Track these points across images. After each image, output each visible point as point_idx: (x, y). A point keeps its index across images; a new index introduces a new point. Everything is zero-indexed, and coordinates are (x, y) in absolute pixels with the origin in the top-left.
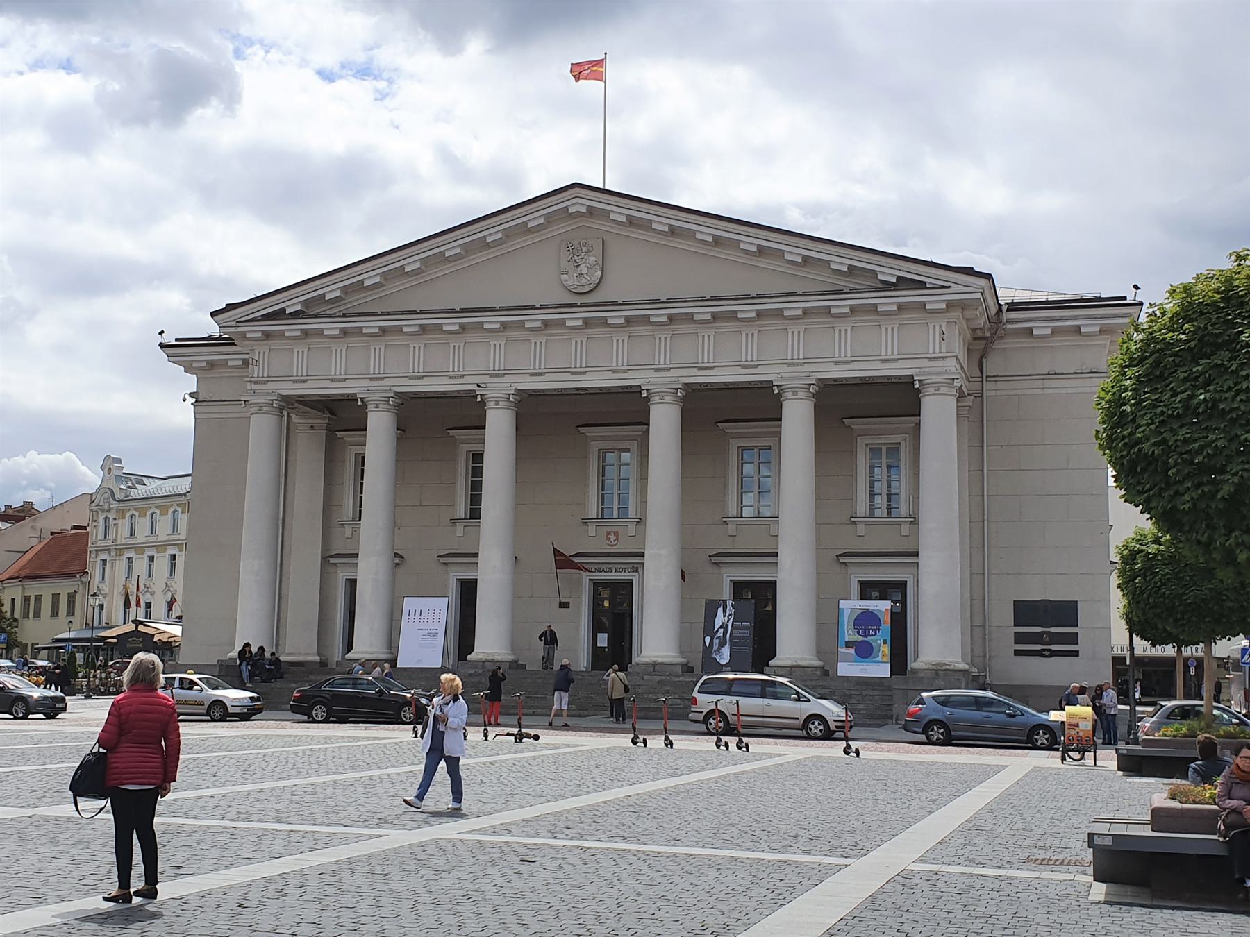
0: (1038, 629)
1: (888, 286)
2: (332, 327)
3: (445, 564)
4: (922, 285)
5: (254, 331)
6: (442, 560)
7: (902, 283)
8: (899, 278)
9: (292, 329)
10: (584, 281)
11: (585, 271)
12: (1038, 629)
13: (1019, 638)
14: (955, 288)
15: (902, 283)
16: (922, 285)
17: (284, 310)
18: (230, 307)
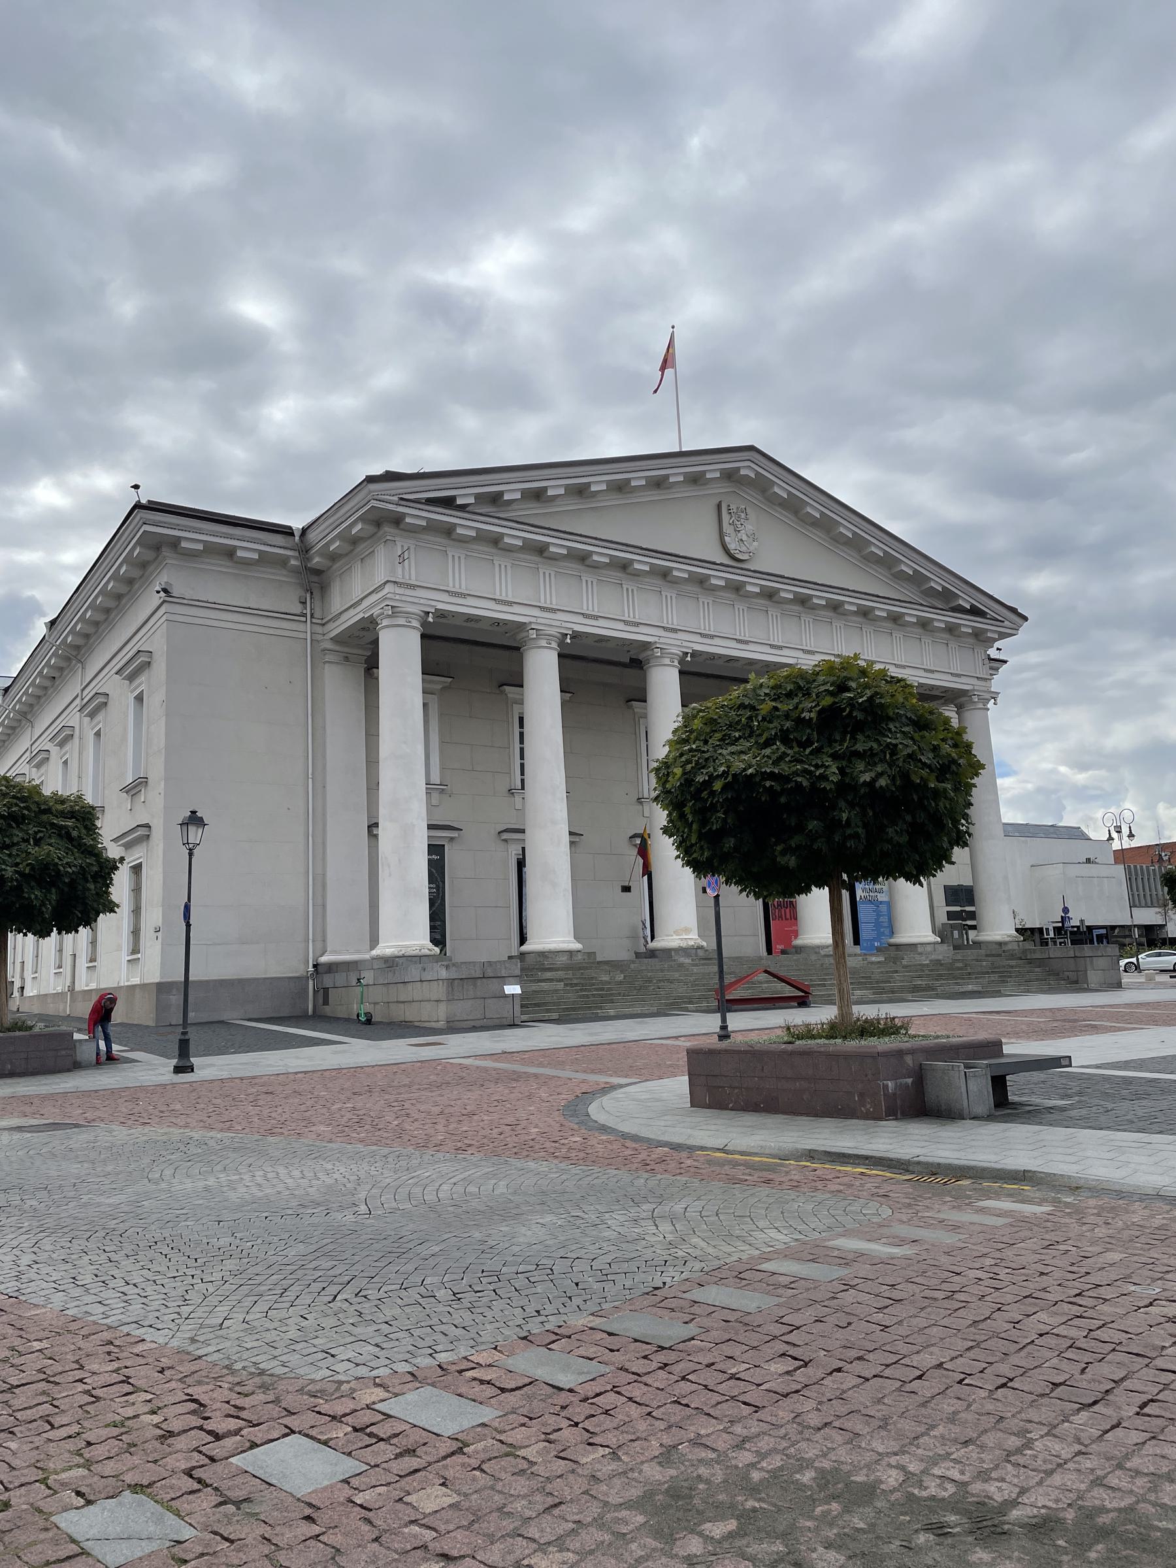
0: (958, 909)
1: (959, 609)
2: (514, 536)
3: (506, 840)
4: (982, 614)
5: (416, 516)
6: (505, 836)
7: (975, 611)
8: (972, 606)
9: (466, 526)
10: (744, 549)
11: (744, 538)
12: (958, 909)
13: (951, 915)
14: (1007, 623)
15: (975, 611)
16: (982, 614)
17: (453, 498)
18: (390, 477)
